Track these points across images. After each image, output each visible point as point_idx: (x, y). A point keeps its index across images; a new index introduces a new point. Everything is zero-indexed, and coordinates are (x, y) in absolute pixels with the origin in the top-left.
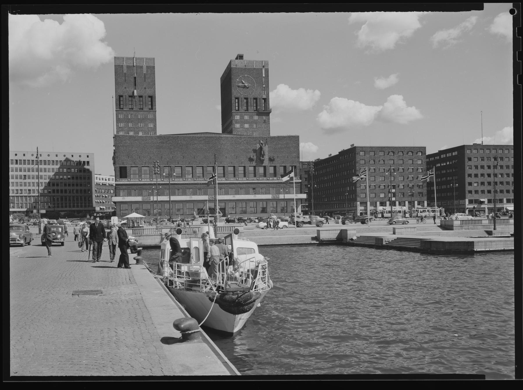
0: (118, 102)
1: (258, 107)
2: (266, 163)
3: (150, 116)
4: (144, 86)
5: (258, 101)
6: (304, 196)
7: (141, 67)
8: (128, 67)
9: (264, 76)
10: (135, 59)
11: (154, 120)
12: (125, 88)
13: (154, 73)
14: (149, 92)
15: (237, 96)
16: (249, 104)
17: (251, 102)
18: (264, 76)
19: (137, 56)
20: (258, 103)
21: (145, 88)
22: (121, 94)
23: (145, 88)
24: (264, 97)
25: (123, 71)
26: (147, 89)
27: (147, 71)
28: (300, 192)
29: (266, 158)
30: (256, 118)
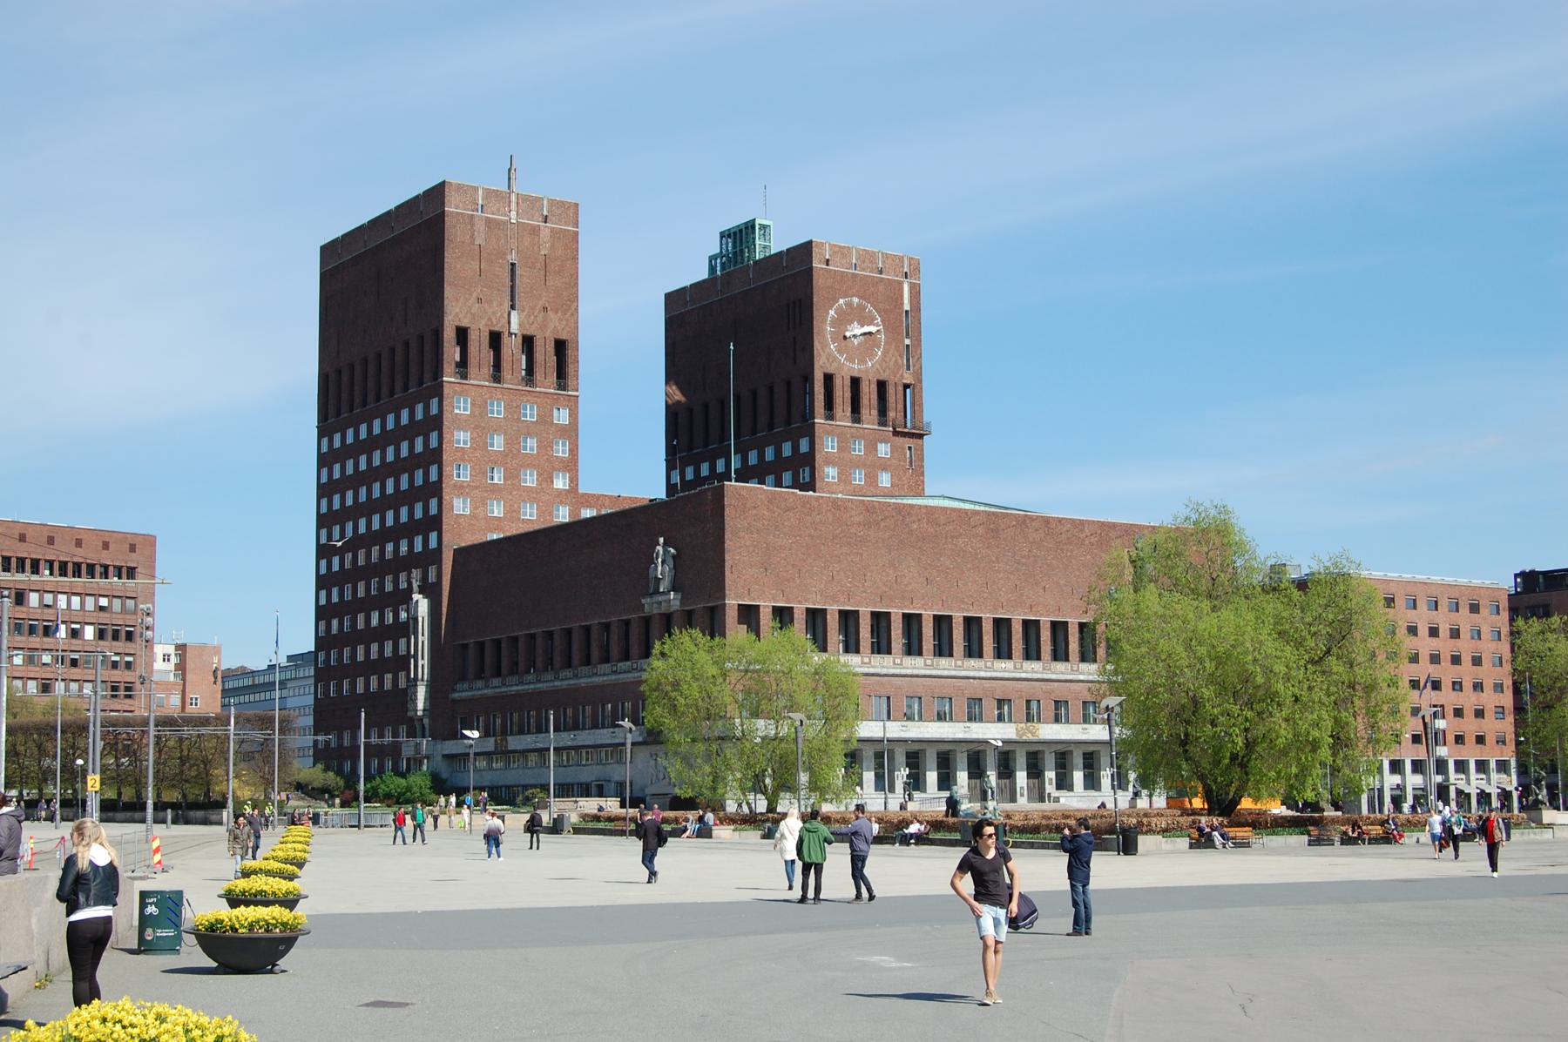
1: (891, 414)
3: (562, 417)
4: (541, 303)
7: (535, 231)
9: (907, 307)
11: (571, 432)
12: (479, 300)
13: (575, 259)
15: (830, 370)
17: (869, 394)
18: (907, 307)
19: (524, 186)
21: (545, 309)
27: (553, 246)
30: (883, 450)
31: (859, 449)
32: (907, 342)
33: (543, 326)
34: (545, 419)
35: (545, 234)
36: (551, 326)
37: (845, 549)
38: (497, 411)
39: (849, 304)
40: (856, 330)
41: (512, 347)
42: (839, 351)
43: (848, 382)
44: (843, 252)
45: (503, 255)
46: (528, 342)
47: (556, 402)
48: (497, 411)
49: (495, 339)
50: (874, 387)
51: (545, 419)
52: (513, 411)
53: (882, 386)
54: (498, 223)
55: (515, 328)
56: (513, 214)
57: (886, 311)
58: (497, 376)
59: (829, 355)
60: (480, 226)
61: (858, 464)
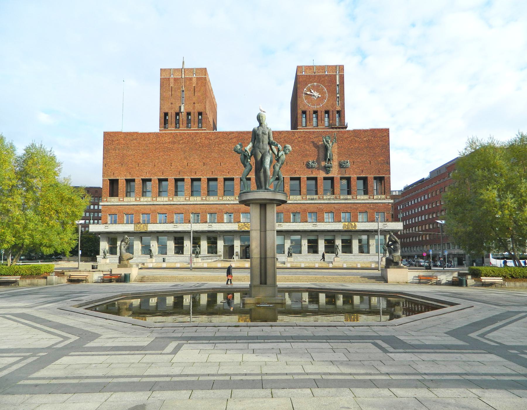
0: (163, 120)
2: (335, 173)
5: (331, 113)
6: (399, 226)
7: (191, 79)
8: (175, 80)
10: (183, 70)
12: (172, 104)
14: (199, 107)
15: (304, 109)
16: (319, 118)
18: (338, 83)
20: (331, 116)
22: (166, 111)
23: (194, 103)
24: (338, 108)
25: (169, 84)
26: (196, 105)
27: (197, 84)
28: (391, 219)
29: (335, 164)
32: (338, 95)
33: (194, 108)
35: (194, 80)
36: (196, 108)
37: (162, 153)
39: (313, 86)
41: (183, 117)
42: (308, 102)
45: (179, 89)
46: (189, 114)
49: (177, 114)
50: (323, 113)
54: (178, 79)
55: (182, 110)
56: (183, 75)
57: (329, 86)
59: (304, 105)
60: (172, 81)
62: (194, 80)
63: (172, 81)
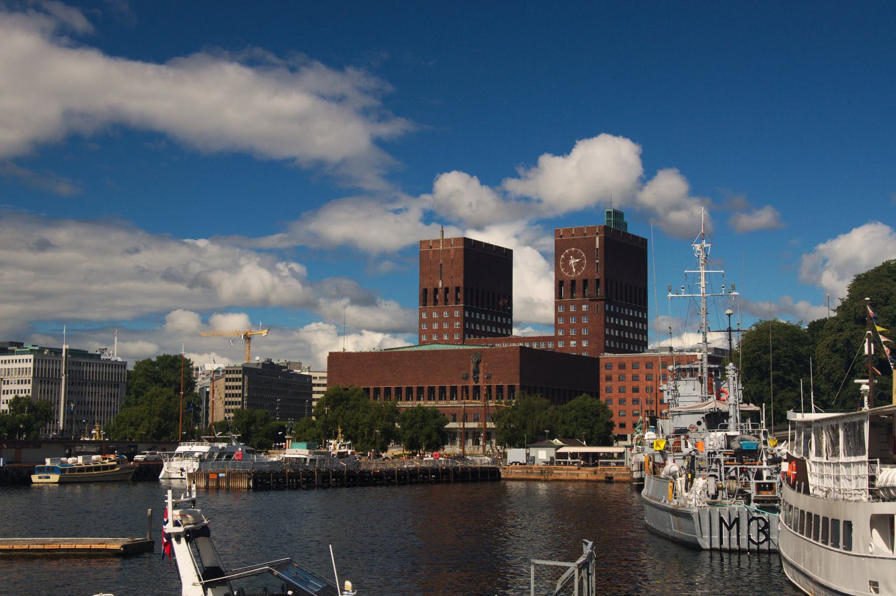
29: (481, 375)
31: (572, 309)
34: (451, 315)
38: (435, 315)
39: (570, 251)
40: (573, 261)
43: (569, 283)
44: (568, 231)
46: (447, 290)
47: (455, 308)
48: (435, 315)
49: (436, 291)
51: (451, 315)
52: (440, 314)
53: (585, 282)
58: (436, 302)
59: (562, 274)
61: (573, 314)
62: (452, 252)
63: (431, 253)
